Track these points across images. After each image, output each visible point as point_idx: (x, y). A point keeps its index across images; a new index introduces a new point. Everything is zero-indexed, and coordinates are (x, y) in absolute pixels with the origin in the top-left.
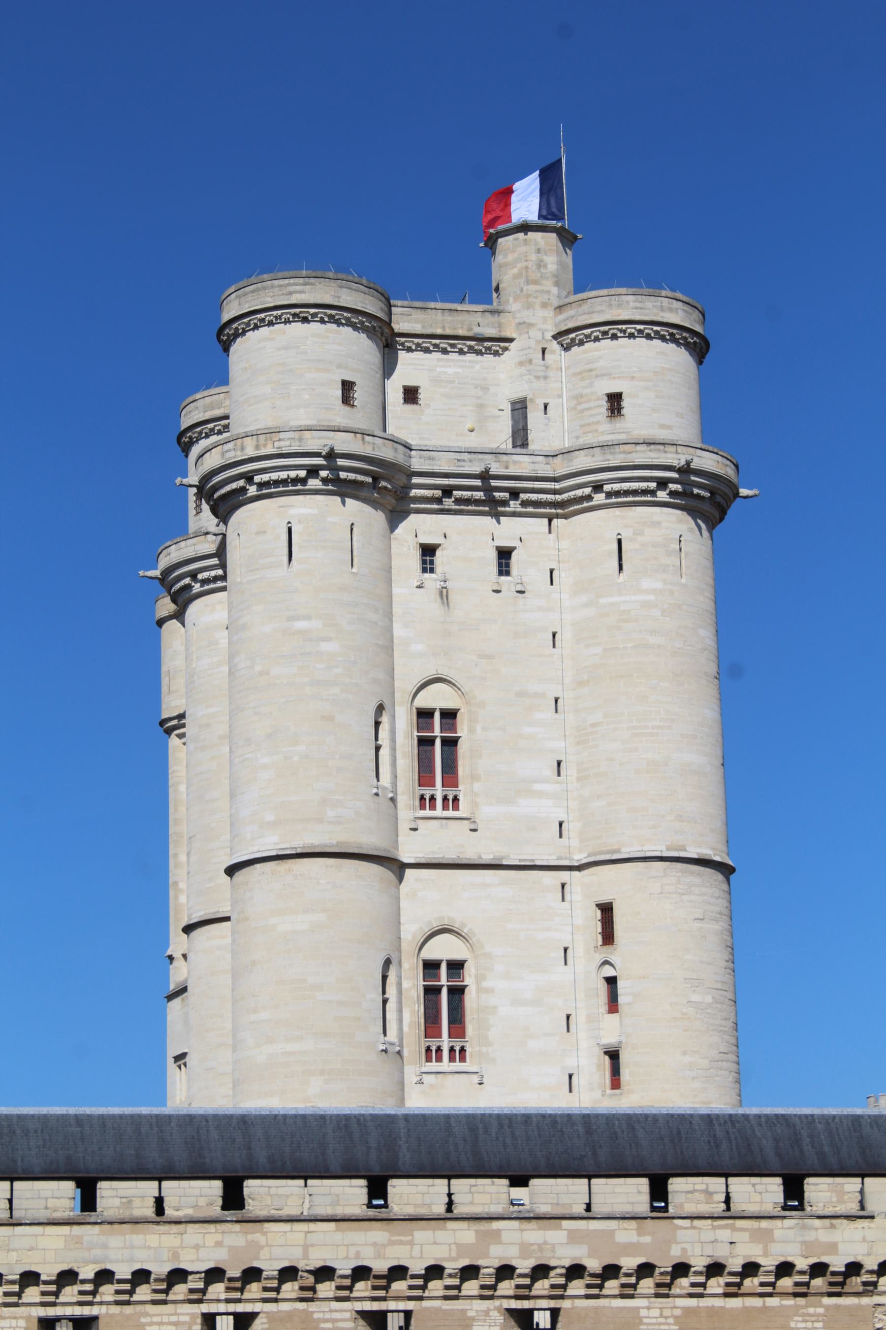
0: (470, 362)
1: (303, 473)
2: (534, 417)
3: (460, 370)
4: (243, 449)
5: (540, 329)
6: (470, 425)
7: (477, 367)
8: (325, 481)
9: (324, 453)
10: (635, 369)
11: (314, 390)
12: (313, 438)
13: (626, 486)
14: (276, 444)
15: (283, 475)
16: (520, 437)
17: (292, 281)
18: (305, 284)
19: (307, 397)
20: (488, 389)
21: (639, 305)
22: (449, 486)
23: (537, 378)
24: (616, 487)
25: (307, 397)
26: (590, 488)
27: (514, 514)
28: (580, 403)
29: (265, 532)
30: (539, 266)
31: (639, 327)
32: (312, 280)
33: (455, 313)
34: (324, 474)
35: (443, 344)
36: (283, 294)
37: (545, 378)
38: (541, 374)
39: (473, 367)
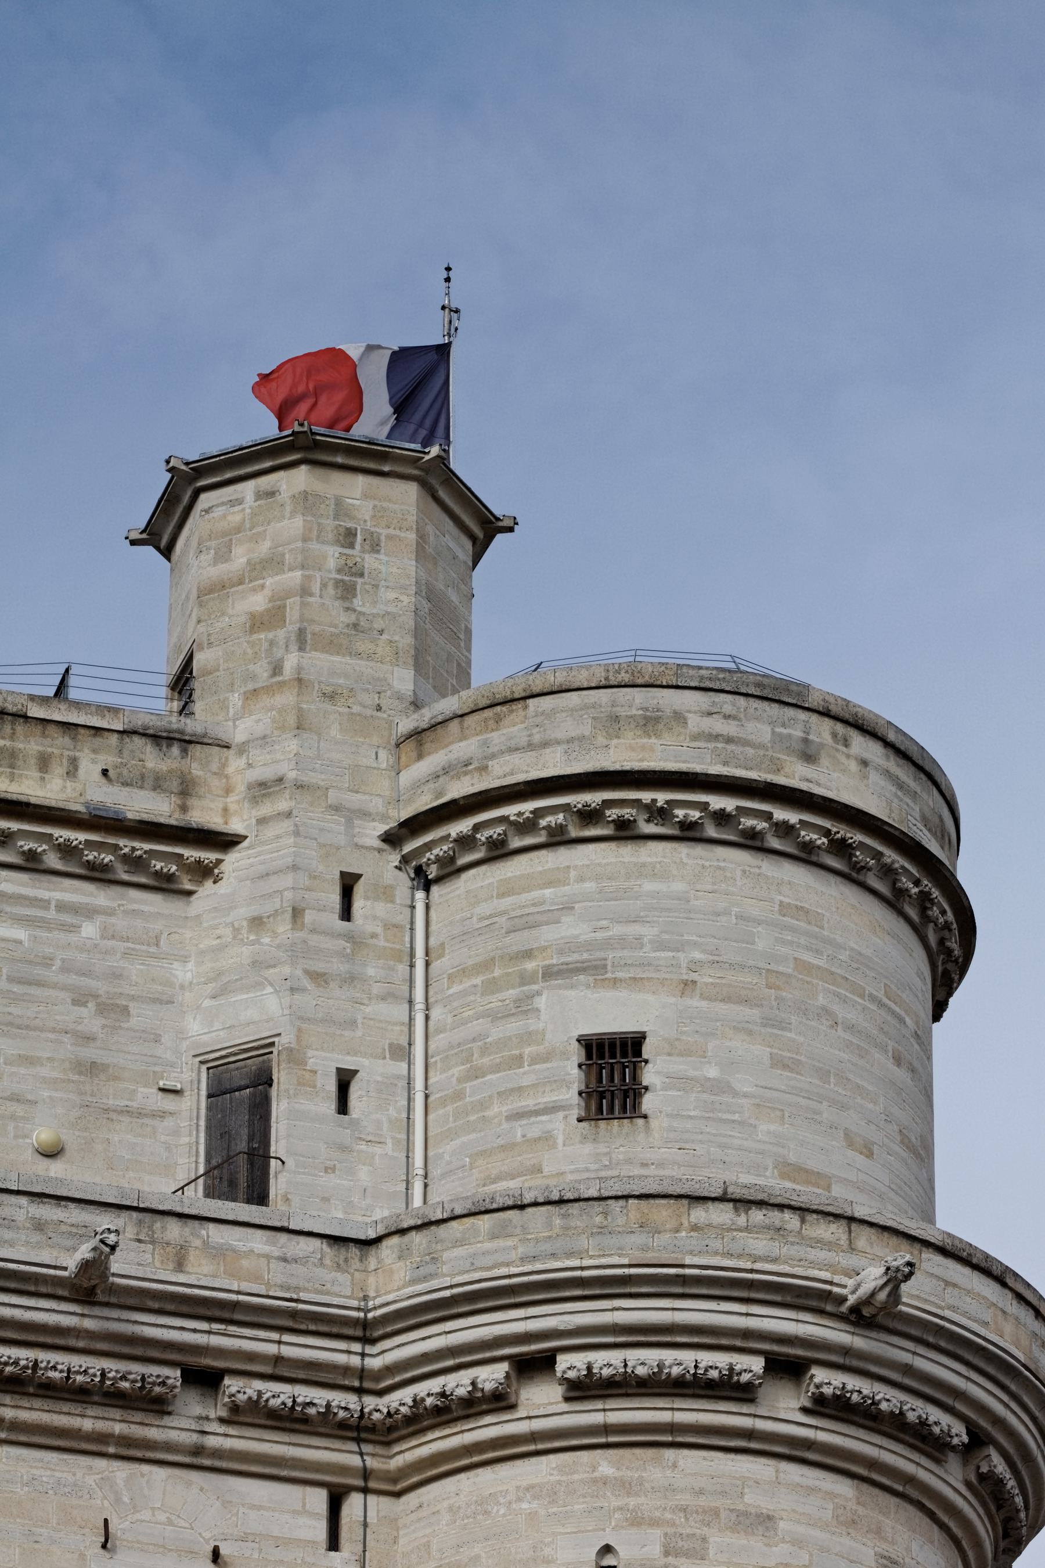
0: (61, 907)
2: (296, 1118)
3: (20, 934)
5: (337, 809)
6: (43, 1135)
7: (89, 930)
10: (697, 955)
13: (643, 1360)
16: (241, 1166)
20: (125, 1010)
21: (719, 726)
23: (318, 978)
24: (607, 1362)
26: (504, 1367)
27: (199, 1460)
28: (476, 1073)
30: (347, 592)
31: (718, 802)
33: (20, 728)
37: (350, 979)
38: (337, 967)
39: (74, 928)
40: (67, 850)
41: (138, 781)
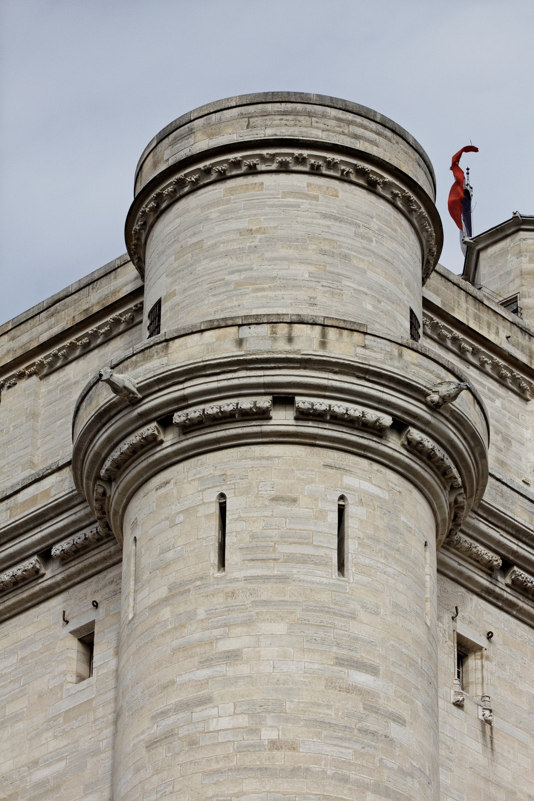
1: (387, 420)
4: (290, 340)
8: (413, 447)
9: (435, 398)
11: (379, 301)
12: (419, 365)
14: (360, 350)
15: (355, 411)
17: (359, 119)
18: (378, 134)
19: (370, 307)
22: (515, 553)
25: (370, 307)
29: (294, 500)
32: (389, 134)
34: (416, 434)
35: (468, 343)
36: (343, 133)
40: (495, 366)
41: (516, 345)
